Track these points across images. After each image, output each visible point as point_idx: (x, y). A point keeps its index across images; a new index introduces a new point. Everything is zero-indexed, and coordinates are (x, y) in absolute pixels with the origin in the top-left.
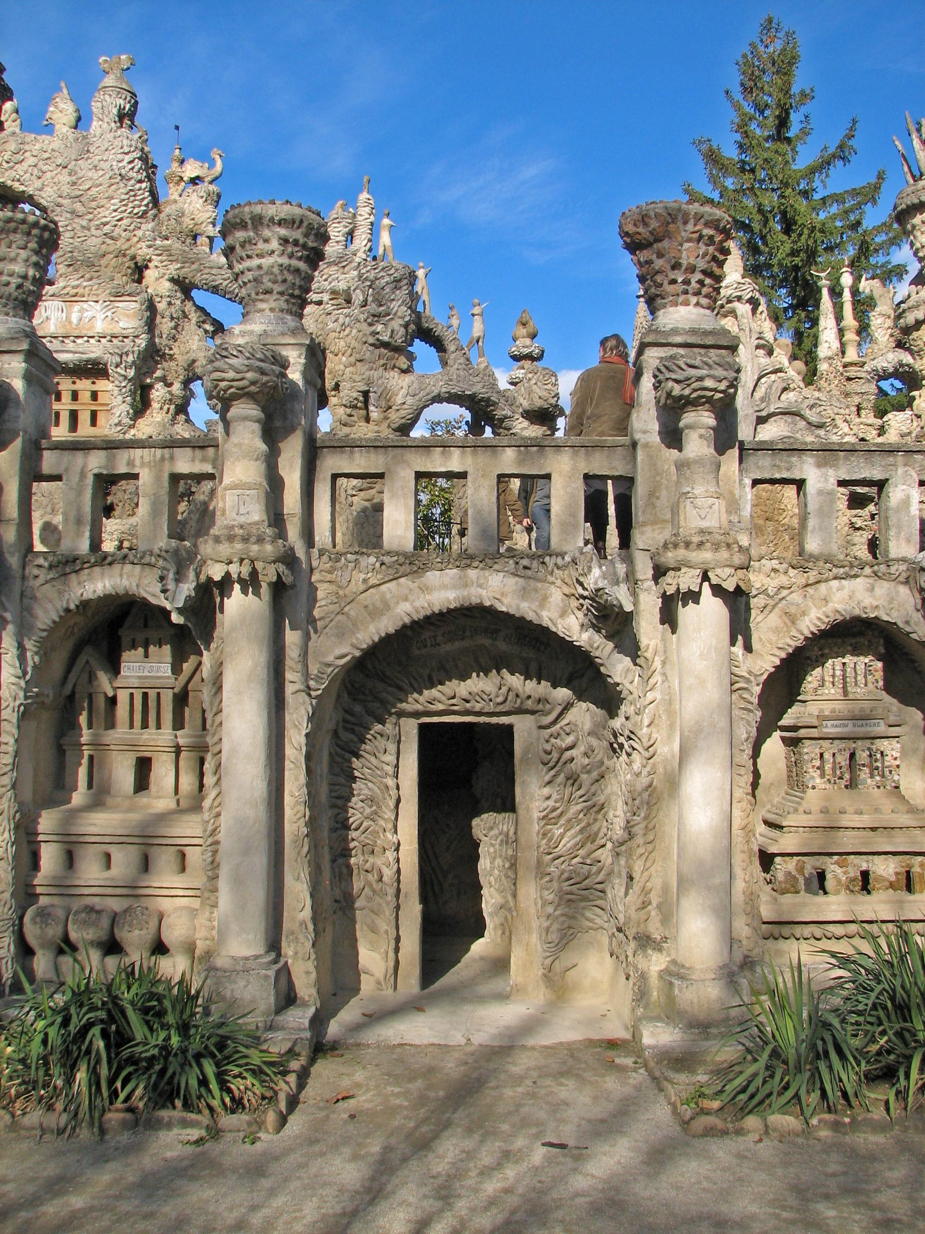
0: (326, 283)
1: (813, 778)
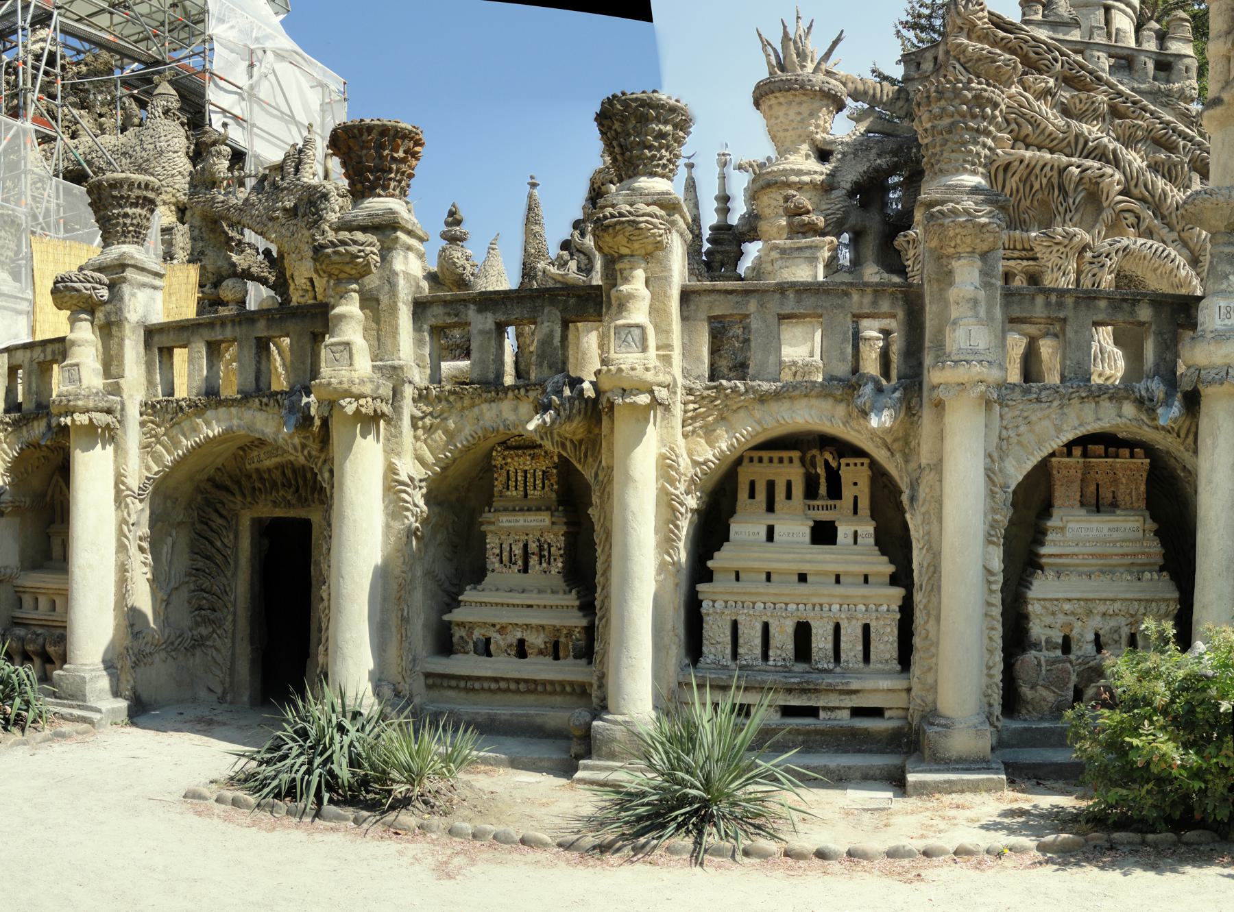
1: (493, 563)
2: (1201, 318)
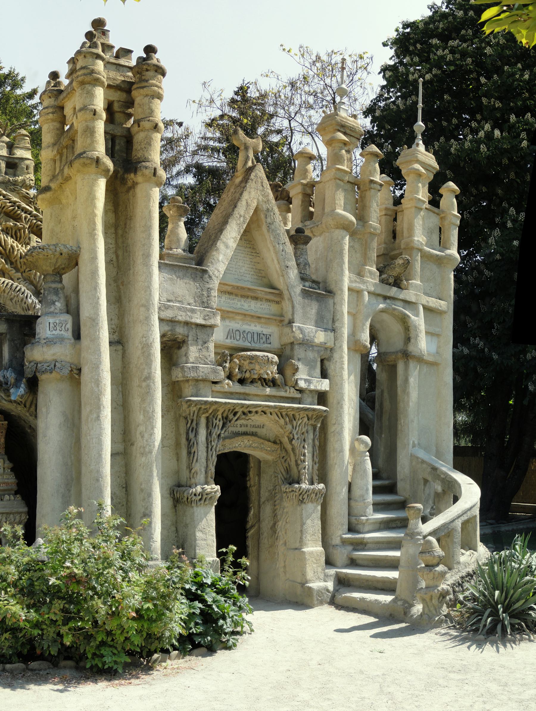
2: (38, 331)
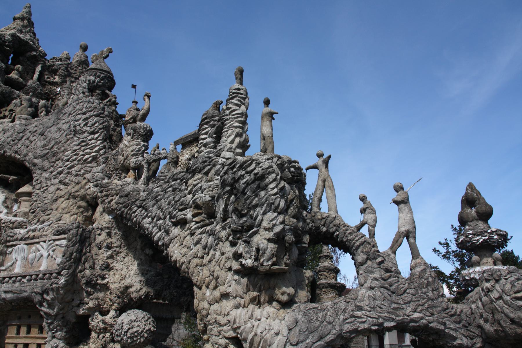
0: (190, 196)
